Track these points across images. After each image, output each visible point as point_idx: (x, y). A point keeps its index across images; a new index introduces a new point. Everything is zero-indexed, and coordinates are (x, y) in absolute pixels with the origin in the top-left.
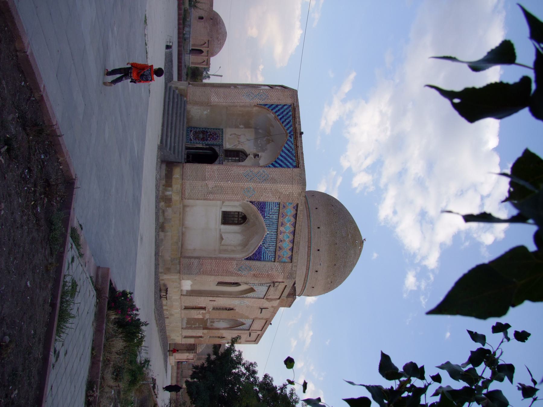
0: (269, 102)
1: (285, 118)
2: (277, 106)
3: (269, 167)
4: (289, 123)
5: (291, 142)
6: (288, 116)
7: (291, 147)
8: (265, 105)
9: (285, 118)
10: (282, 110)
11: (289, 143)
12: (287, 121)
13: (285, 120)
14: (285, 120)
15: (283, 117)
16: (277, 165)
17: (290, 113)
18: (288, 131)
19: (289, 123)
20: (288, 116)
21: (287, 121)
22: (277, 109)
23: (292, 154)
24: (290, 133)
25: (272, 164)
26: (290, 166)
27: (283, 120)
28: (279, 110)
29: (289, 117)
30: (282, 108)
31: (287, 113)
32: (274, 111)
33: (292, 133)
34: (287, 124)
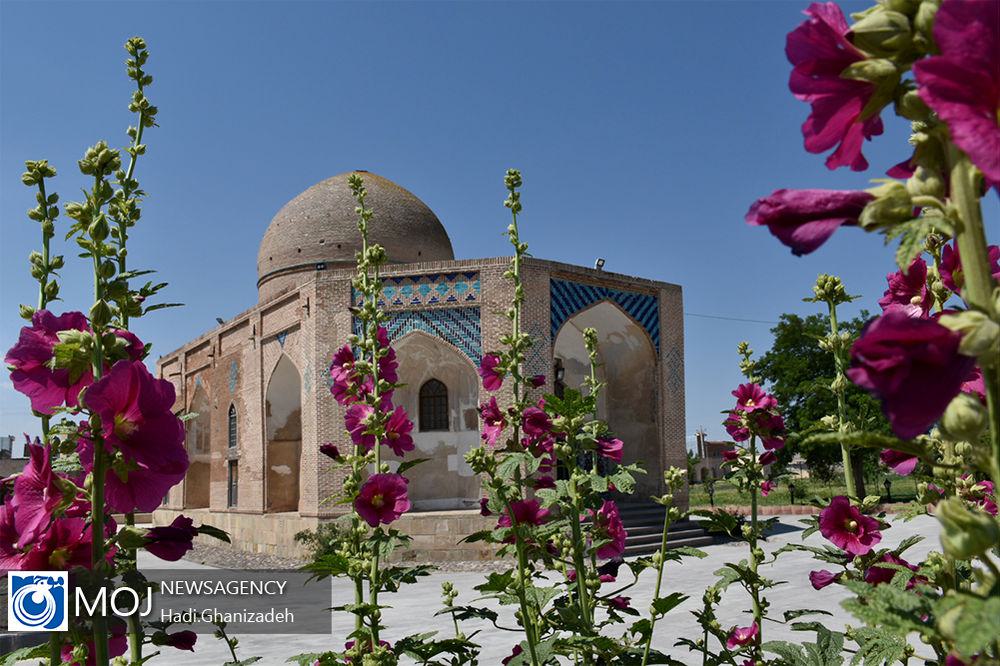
0: (547, 326)
1: (576, 297)
2: (553, 309)
3: (658, 344)
4: (585, 291)
5: (619, 295)
6: (571, 290)
7: (627, 298)
8: (552, 335)
9: (576, 297)
10: (560, 298)
11: (621, 299)
12: (582, 294)
13: (580, 297)
14: (580, 297)
15: (573, 300)
16: (654, 330)
17: (567, 285)
18: (602, 297)
19: (585, 291)
20: (571, 290)
21: (582, 294)
22: (557, 308)
23: (638, 298)
24: (604, 295)
25: (653, 339)
26: (655, 305)
27: (580, 302)
28: (561, 307)
29: (575, 288)
30: (558, 302)
31: (567, 290)
32: (562, 316)
33: (604, 290)
34: (587, 295)
